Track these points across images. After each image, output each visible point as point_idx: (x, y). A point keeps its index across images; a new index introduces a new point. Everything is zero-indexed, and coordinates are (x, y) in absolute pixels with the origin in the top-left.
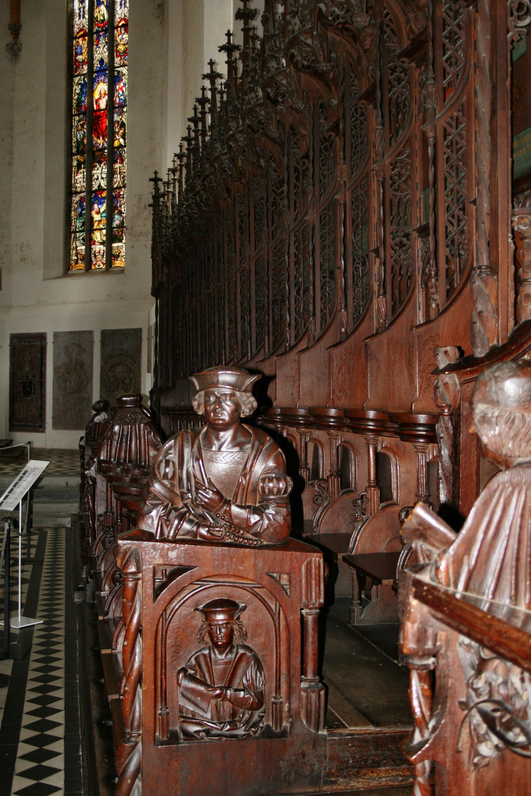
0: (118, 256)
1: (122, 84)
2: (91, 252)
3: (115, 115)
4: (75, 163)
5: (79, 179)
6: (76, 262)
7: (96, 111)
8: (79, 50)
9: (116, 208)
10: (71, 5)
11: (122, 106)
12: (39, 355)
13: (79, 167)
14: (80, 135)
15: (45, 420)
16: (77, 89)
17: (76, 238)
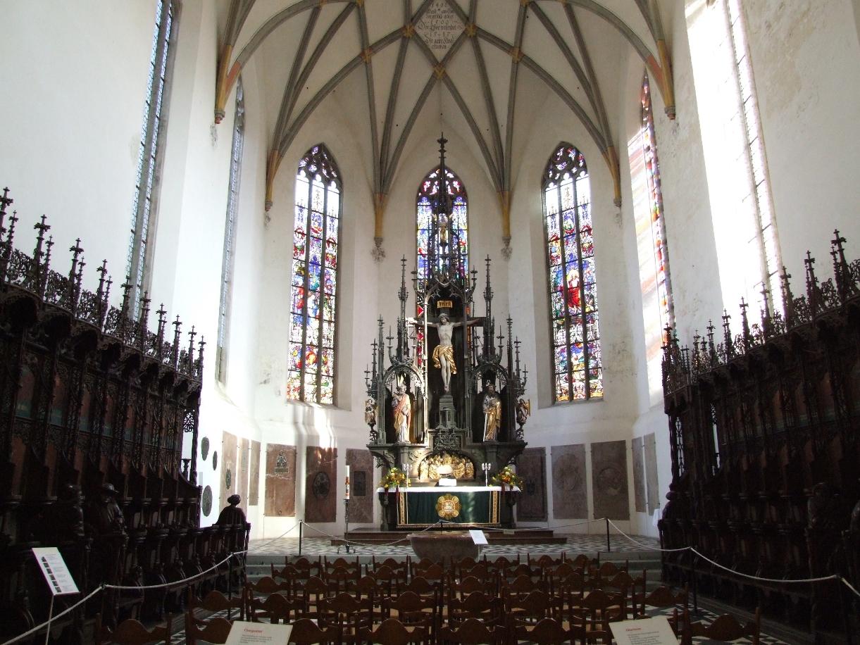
0: (595, 389)
1: (588, 269)
2: (572, 388)
3: (585, 291)
4: (555, 326)
5: (560, 337)
6: (561, 395)
7: (570, 289)
8: (553, 250)
9: (591, 354)
10: (545, 220)
11: (590, 284)
12: (540, 464)
13: (559, 327)
14: (558, 307)
15: (547, 512)
16: (553, 275)
17: (559, 378)
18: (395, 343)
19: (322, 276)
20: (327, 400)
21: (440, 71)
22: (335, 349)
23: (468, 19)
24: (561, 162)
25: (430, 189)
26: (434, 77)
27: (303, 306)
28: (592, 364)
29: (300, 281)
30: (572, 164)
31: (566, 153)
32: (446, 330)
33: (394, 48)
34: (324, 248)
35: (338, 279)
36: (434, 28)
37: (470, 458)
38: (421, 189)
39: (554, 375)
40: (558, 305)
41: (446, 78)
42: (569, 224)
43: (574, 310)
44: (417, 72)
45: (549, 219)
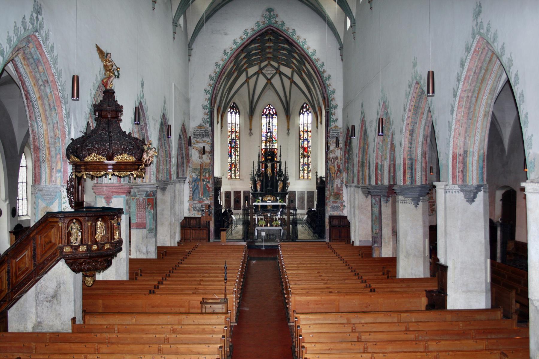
5: (302, 160)
16: (301, 142)
18: (257, 168)
19: (235, 142)
20: (237, 177)
21: (269, 80)
22: (239, 163)
23: (277, 69)
24: (305, 108)
25: (266, 112)
26: (267, 83)
27: (231, 152)
28: (309, 170)
29: (230, 145)
30: (308, 110)
31: (306, 106)
32: (269, 165)
33: (255, 77)
34: (235, 134)
35: (239, 142)
36: (267, 70)
37: (275, 196)
38: (263, 112)
39: (300, 171)
40: (302, 151)
41: (271, 84)
42: (306, 128)
43: (306, 153)
44: (262, 81)
45: (301, 125)
